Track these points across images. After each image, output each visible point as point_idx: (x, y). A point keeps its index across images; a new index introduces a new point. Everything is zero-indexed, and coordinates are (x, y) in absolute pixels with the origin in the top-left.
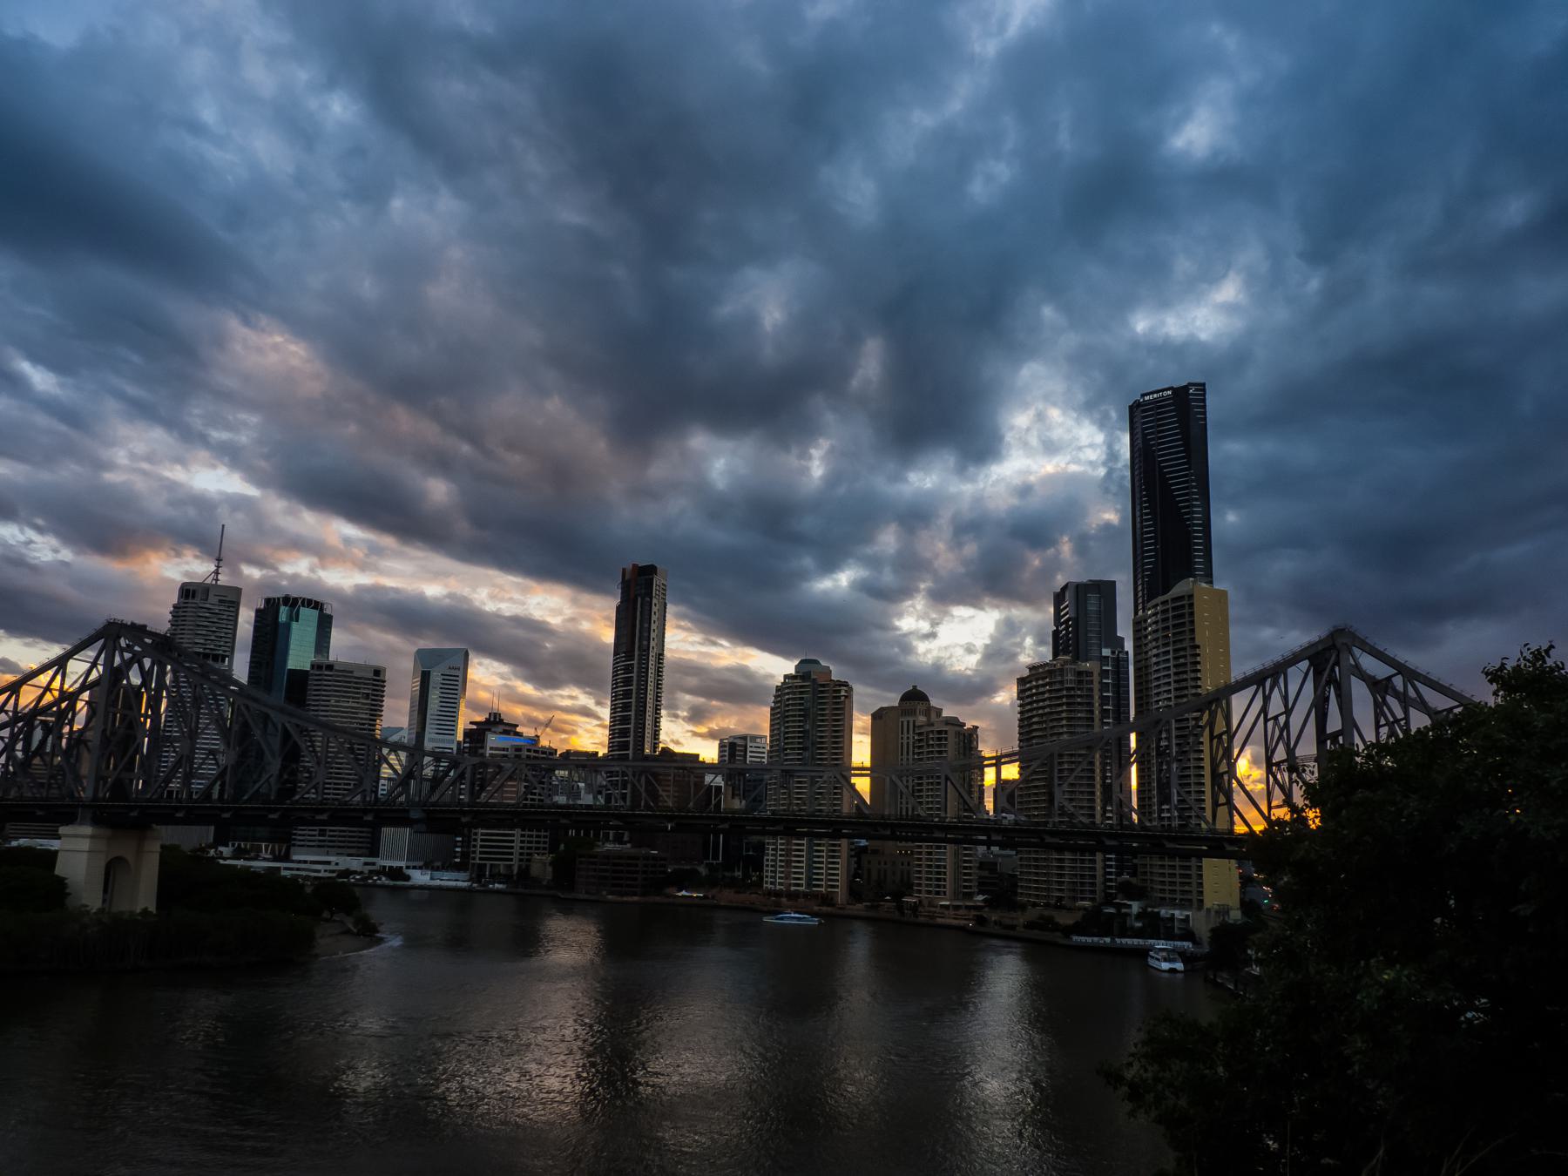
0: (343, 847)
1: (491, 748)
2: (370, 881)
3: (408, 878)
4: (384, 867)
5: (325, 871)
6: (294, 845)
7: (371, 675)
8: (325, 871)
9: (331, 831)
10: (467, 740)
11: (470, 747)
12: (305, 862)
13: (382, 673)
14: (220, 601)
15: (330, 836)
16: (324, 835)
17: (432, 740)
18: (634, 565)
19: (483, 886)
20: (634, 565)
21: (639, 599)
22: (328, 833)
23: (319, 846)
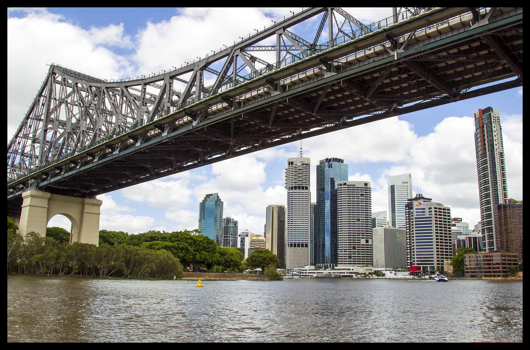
0: (360, 264)
1: (416, 209)
2: (368, 277)
3: (384, 275)
4: (375, 271)
5: (347, 273)
6: (339, 263)
7: (363, 186)
8: (347, 273)
9: (353, 256)
10: (407, 208)
11: (409, 212)
12: (340, 269)
13: (368, 185)
14: (302, 164)
15: (353, 259)
16: (351, 259)
17: (398, 216)
18: (479, 110)
19: (420, 277)
20: (479, 110)
21: (485, 125)
22: (352, 258)
23: (349, 264)
